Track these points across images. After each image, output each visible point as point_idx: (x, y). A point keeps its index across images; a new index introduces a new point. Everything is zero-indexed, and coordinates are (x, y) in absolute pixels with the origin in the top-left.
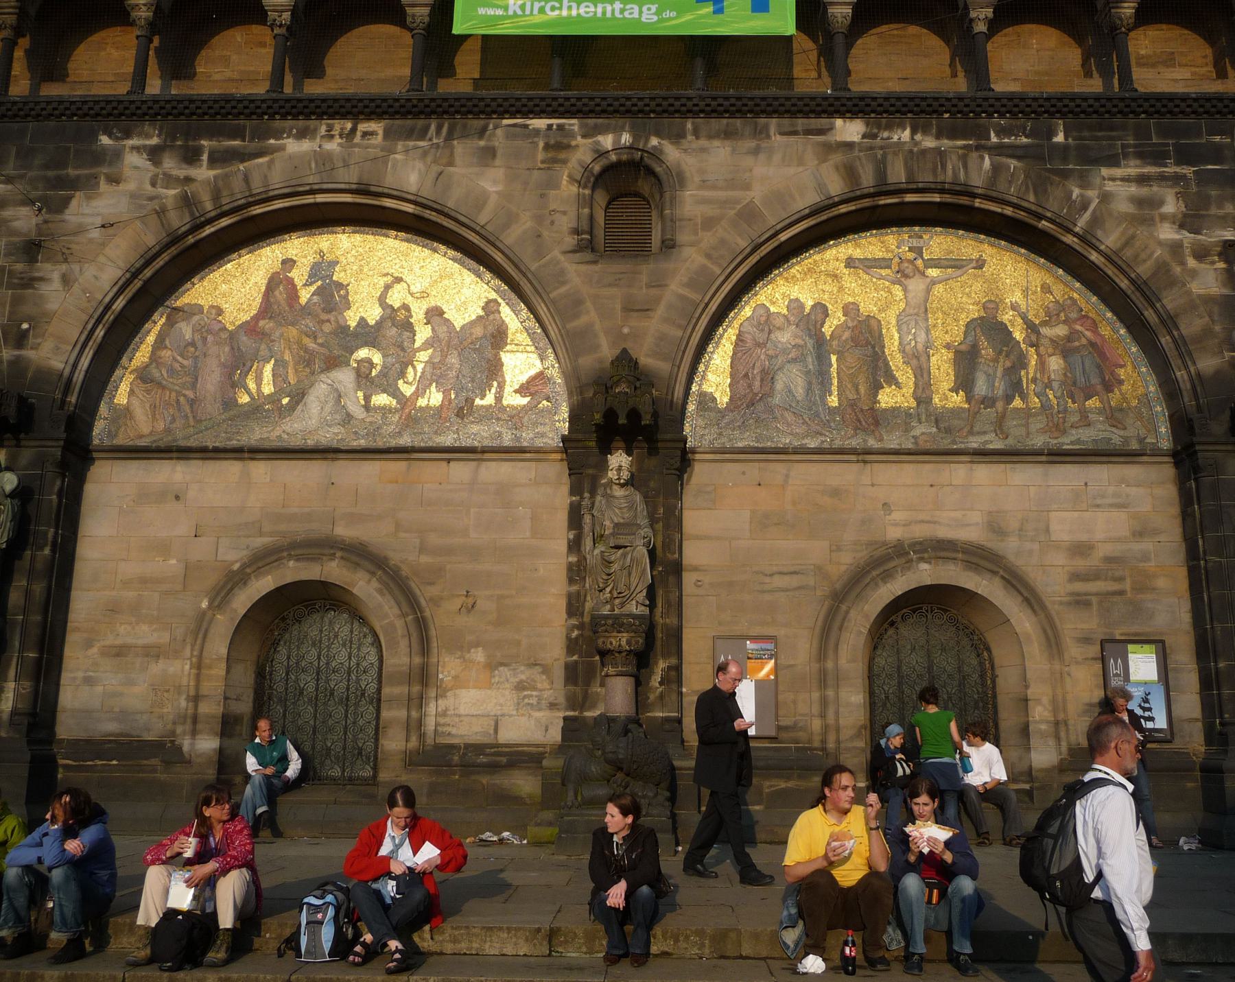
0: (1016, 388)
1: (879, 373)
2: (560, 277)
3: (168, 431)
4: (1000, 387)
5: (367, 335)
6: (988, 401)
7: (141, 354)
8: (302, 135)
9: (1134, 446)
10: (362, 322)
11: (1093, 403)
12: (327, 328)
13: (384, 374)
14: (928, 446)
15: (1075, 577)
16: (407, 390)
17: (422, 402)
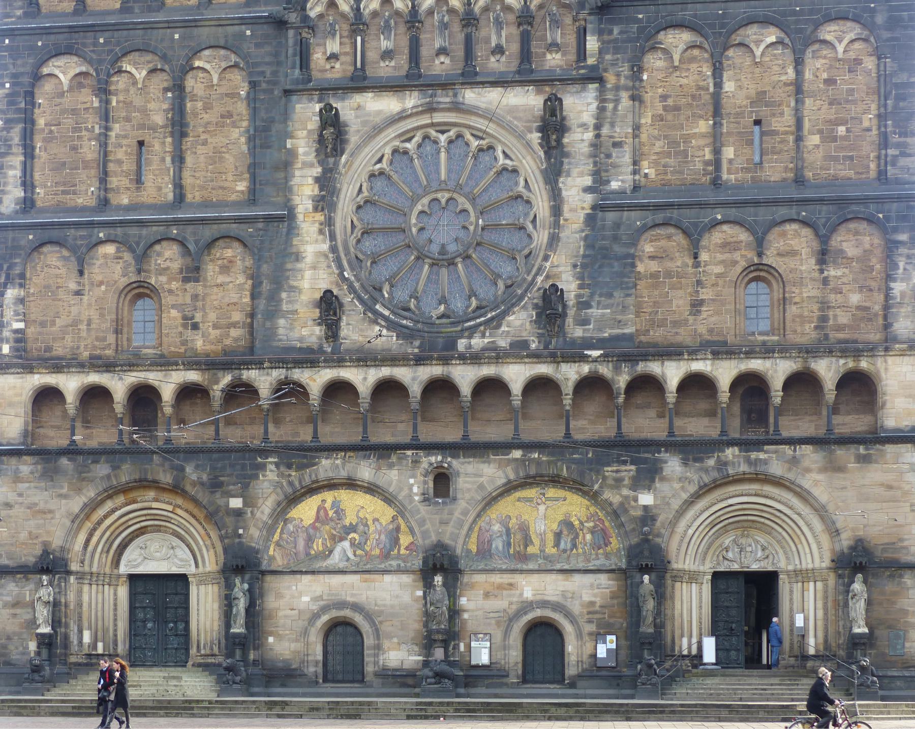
0: (574, 546)
1: (527, 541)
2: (418, 511)
3: (288, 564)
4: (569, 546)
5: (353, 528)
6: (565, 551)
7: (276, 537)
8: (327, 458)
9: (614, 567)
10: (351, 524)
11: (601, 551)
12: (339, 526)
13: (360, 544)
14: (544, 568)
15: (589, 613)
16: (367, 548)
17: (373, 553)
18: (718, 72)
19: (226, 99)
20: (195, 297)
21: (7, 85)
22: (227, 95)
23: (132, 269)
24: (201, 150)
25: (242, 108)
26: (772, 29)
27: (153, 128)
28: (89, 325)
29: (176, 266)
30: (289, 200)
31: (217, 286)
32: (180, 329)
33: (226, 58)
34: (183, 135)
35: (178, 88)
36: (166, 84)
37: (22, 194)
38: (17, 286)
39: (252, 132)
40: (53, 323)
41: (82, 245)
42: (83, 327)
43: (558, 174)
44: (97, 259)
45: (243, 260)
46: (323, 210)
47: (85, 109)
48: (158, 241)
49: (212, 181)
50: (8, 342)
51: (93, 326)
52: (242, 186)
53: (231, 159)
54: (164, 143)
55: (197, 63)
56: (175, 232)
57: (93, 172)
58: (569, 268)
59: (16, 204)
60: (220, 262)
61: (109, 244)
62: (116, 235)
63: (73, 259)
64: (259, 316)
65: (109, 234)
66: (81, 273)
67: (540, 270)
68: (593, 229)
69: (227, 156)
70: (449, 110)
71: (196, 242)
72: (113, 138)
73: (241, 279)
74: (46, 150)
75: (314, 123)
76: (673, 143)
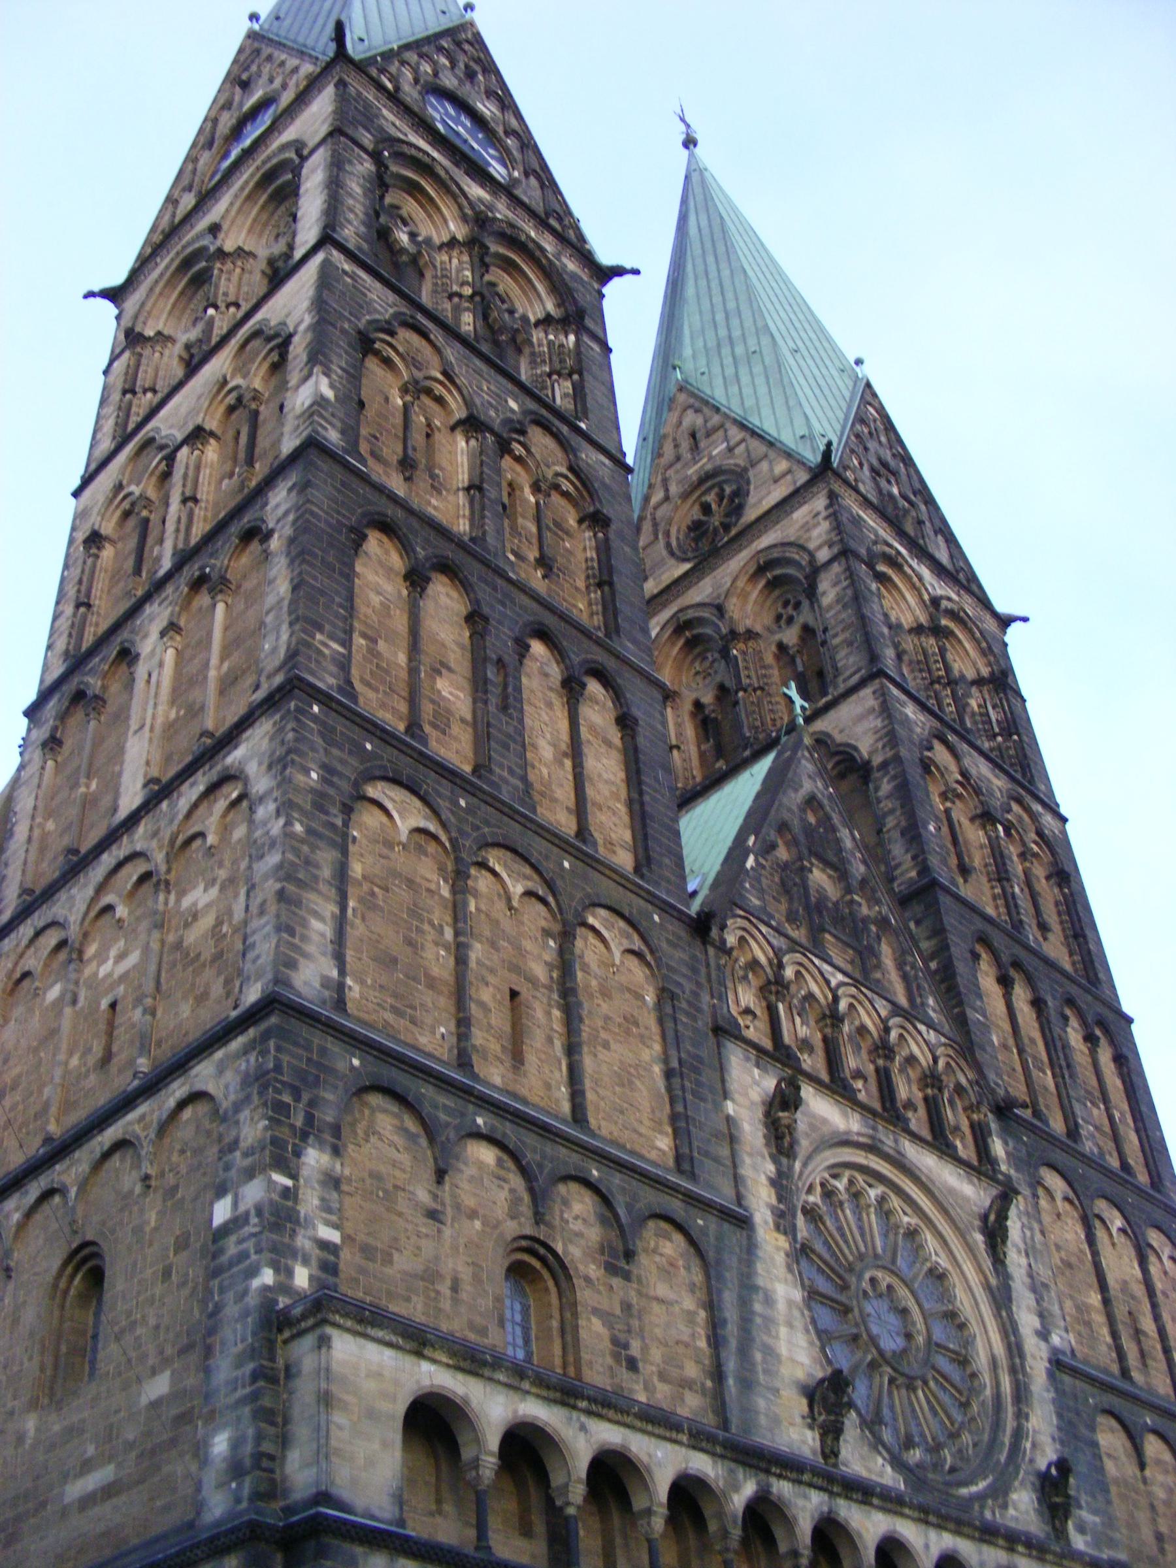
18: (1091, 1240)
19: (627, 995)
20: (627, 1307)
21: (314, 775)
22: (629, 990)
23: (526, 1208)
24: (603, 1054)
25: (650, 1021)
26: (1116, 1213)
27: (532, 981)
28: (455, 1288)
29: (594, 1234)
30: (739, 1199)
31: (657, 1299)
32: (609, 1360)
33: (628, 937)
34: (581, 1020)
35: (566, 937)
36: (544, 923)
37: (335, 973)
38: (328, 1149)
39: (675, 1064)
40: (388, 1260)
41: (447, 1125)
42: (445, 1288)
43: (1010, 1299)
44: (466, 1164)
45: (688, 1268)
46: (785, 1233)
47: (429, 890)
48: (567, 1178)
49: (622, 1112)
50: (306, 1262)
51: (464, 1296)
52: (664, 1143)
53: (645, 1093)
54: (549, 1014)
55: (591, 920)
56: (595, 1173)
57: (445, 1002)
58: (1049, 1440)
59: (322, 985)
60: (657, 1258)
61: (484, 1143)
62: (505, 1134)
63: (424, 1142)
64: (731, 1381)
65: (493, 1128)
66: (440, 1175)
67: (1019, 1434)
68: (1057, 1390)
69: (638, 1083)
70: (886, 1157)
71: (629, 1207)
72: (473, 964)
73: (689, 1303)
74: (363, 919)
75: (756, 1095)
76: (1077, 1307)
